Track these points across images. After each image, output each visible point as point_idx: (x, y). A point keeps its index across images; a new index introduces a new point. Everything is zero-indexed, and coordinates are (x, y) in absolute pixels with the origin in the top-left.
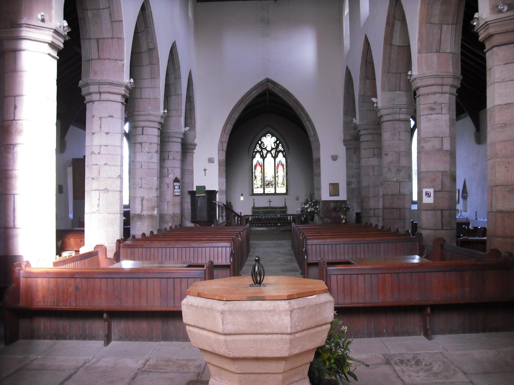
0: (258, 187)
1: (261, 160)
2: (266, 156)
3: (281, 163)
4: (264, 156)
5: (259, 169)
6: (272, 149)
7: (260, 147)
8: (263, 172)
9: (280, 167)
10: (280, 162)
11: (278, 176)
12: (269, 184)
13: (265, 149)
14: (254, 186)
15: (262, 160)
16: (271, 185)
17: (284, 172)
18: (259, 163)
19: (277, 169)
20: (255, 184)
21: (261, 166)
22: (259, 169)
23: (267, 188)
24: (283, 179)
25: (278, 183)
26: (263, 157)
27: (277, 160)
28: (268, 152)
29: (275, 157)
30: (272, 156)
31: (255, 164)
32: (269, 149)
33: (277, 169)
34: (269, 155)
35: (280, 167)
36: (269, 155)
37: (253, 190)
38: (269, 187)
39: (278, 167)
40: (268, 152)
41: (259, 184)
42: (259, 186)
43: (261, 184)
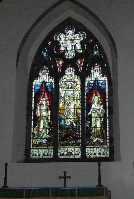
0: (41, 144)
1: (50, 81)
2: (63, 73)
3: (96, 87)
4: (59, 71)
5: (44, 101)
6: (78, 56)
7: (50, 53)
8: (54, 106)
9: (96, 99)
10: (96, 81)
11: (90, 117)
12: (67, 136)
13: (62, 56)
14: (33, 142)
15: (52, 81)
16: (74, 139)
17: (105, 107)
18: (46, 87)
19: (88, 100)
20: (36, 137)
21: (49, 94)
22: (44, 101)
23: (62, 145)
24: (104, 124)
25: (89, 135)
26: (57, 75)
27: (90, 80)
28: (69, 63)
29: (83, 75)
30: (77, 73)
31: (37, 88)
32: (70, 55)
33: (88, 100)
34: (70, 72)
35: (96, 99)
36: (70, 72)
37: (27, 152)
38: (68, 144)
39: (90, 95)
40: (69, 63)
41: (44, 137)
42: (44, 141)
43: (48, 137)
